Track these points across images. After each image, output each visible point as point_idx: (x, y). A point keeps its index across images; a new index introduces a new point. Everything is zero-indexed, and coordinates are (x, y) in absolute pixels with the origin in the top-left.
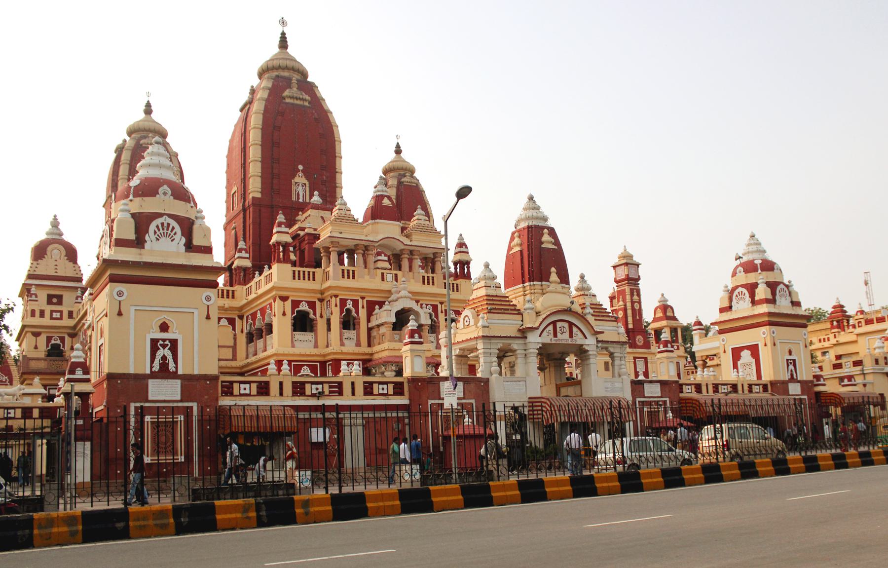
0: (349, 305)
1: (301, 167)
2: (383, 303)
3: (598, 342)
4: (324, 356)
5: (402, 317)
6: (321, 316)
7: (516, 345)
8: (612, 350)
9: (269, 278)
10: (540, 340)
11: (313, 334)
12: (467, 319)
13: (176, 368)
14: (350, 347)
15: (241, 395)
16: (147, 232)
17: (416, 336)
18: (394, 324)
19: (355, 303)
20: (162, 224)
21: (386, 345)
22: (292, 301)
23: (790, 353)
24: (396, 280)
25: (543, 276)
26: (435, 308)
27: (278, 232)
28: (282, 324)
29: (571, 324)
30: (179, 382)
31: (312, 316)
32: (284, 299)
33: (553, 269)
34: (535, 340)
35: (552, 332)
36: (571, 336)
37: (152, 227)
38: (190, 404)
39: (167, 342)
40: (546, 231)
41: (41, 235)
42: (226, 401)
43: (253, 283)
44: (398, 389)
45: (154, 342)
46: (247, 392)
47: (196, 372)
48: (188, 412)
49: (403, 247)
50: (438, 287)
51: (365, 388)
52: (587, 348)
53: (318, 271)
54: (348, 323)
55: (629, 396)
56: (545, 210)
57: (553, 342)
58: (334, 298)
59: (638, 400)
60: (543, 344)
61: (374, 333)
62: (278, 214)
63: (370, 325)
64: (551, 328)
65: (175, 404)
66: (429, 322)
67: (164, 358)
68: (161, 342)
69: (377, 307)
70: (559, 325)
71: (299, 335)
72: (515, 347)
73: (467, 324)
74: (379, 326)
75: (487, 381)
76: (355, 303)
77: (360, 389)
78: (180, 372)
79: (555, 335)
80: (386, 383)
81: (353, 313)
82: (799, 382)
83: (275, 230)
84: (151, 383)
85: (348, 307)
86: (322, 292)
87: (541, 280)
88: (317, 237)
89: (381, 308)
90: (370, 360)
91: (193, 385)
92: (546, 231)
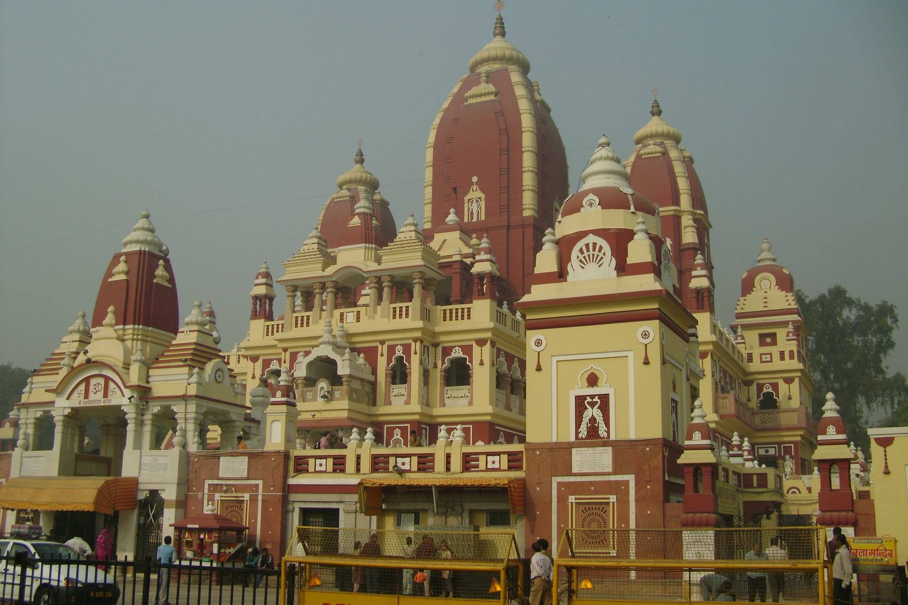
18: (306, 379)
23: (593, 380)
32: (254, 359)
35: (83, 392)
50: (413, 319)
57: (82, 405)
60: (72, 409)
64: (82, 387)
70: (93, 382)
82: (606, 443)
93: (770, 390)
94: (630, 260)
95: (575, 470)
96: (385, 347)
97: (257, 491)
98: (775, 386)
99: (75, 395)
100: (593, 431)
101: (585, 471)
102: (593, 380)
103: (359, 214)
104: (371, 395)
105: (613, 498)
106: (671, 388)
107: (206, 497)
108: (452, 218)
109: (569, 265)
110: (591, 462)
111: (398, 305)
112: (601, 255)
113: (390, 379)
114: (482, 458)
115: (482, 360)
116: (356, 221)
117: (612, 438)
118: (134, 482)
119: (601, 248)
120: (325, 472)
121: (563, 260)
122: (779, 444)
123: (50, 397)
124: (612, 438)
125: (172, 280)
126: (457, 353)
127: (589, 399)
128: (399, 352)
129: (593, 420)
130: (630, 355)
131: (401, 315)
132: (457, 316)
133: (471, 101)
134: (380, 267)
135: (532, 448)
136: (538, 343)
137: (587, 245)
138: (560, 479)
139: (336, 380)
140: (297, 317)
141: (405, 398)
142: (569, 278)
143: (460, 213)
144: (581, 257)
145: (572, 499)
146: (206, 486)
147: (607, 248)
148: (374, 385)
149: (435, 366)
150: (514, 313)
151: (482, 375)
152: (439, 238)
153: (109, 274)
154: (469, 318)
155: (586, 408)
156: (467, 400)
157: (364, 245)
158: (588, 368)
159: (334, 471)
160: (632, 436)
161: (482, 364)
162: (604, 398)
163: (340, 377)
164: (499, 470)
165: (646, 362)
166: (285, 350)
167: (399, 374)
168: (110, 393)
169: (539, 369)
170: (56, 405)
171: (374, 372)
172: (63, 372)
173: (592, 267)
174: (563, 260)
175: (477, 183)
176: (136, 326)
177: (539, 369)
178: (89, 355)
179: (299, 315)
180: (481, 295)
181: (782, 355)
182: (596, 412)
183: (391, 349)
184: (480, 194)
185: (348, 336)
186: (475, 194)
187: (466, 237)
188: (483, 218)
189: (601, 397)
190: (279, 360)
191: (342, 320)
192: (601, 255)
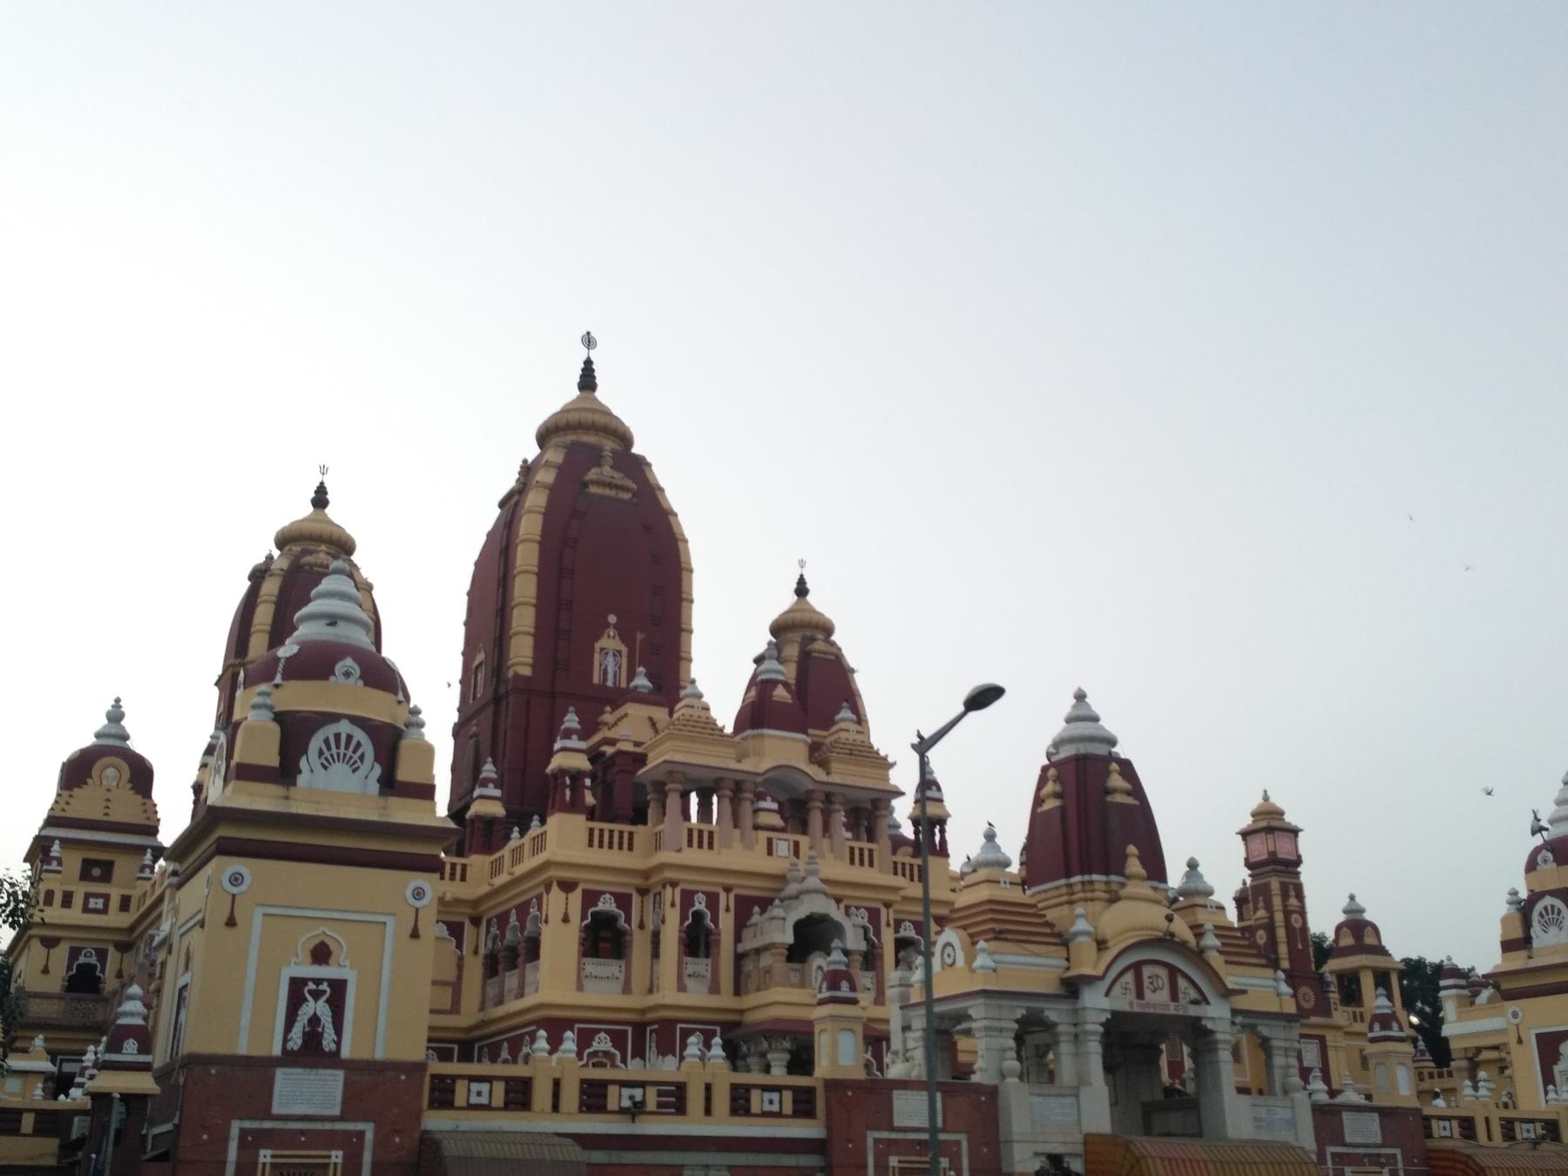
0: (700, 904)
1: (612, 619)
2: (770, 901)
3: (1235, 1012)
4: (643, 1011)
5: (812, 935)
6: (641, 926)
7: (1053, 1013)
8: (1265, 1031)
9: (539, 843)
10: (1106, 1004)
11: (623, 963)
12: (949, 950)
13: (338, 1043)
14: (697, 996)
15: (472, 1107)
16: (305, 751)
17: (845, 985)
18: (790, 948)
19: (712, 900)
20: (337, 736)
21: (777, 994)
22: (585, 892)
24: (797, 853)
25: (1112, 864)
26: (874, 915)
27: (564, 749)
28: (560, 939)
29: (1173, 972)
30: (340, 1075)
31: (622, 922)
33: (1132, 849)
34: (1097, 1004)
35: (1132, 986)
36: (1174, 996)
37: (316, 742)
38: (360, 1126)
39: (324, 986)
40: (1114, 766)
42: (436, 1121)
43: (506, 852)
44: (804, 1105)
45: (297, 985)
46: (484, 1100)
47: (379, 1055)
48: (352, 1144)
49: (810, 786)
50: (881, 871)
51: (734, 1099)
52: (1210, 1025)
53: (639, 829)
54: (697, 941)
55: (1307, 1139)
56: (1109, 724)
57: (1136, 1009)
58: (669, 889)
59: (1330, 1149)
60: (1115, 1014)
61: (748, 966)
62: (565, 713)
63: (741, 949)
64: (1129, 977)
65: (328, 1126)
66: (863, 946)
67: (315, 1020)
68: (311, 986)
69: (756, 909)
70: (1147, 971)
71: (592, 966)
72: (1052, 1016)
73: (949, 961)
74: (758, 951)
75: (993, 1092)
76: (712, 900)
77: (722, 1100)
78: (346, 1053)
79: (1140, 994)
80: (778, 1089)
81: (708, 922)
83: (557, 746)
84: (281, 1074)
85: (697, 907)
86: (646, 874)
87: (1107, 872)
88: (641, 759)
89: (763, 911)
90: (738, 1024)
91: (371, 1083)
92: (1114, 766)
97: (1396, 1163)
99: (1117, 990)
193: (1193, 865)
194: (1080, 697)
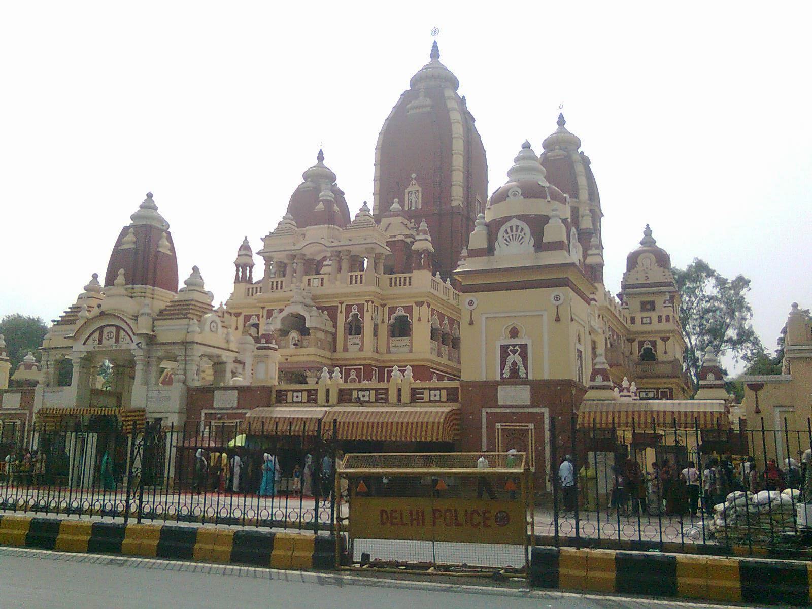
10: (83, 348)
18: (280, 330)
23: (514, 333)
36: (117, 341)
41: (635, 246)
60: (88, 352)
64: (97, 334)
70: (106, 330)
79: (100, 342)
82: (525, 382)
93: (649, 346)
94: (545, 240)
95: (500, 403)
96: (344, 306)
98: (654, 343)
99: (90, 341)
100: (514, 372)
101: (508, 404)
102: (514, 333)
103: (322, 201)
104: (332, 344)
105: (531, 426)
106: (577, 341)
107: (202, 423)
108: (396, 206)
109: (496, 243)
110: (513, 397)
111: (353, 274)
112: (522, 235)
113: (347, 332)
114: (426, 392)
115: (419, 318)
116: (321, 206)
117: (530, 378)
118: (142, 411)
119: (522, 229)
120: (301, 402)
121: (492, 237)
122: (657, 389)
123: (68, 343)
124: (530, 378)
125: (172, 249)
126: (401, 312)
127: (511, 348)
128: (355, 310)
129: (514, 364)
130: (545, 314)
131: (356, 282)
132: (400, 283)
133: (411, 112)
134: (341, 244)
135: (466, 385)
136: (471, 303)
137: (511, 227)
138: (489, 410)
139: (304, 331)
140: (272, 282)
141: (359, 346)
142: (496, 253)
143: (402, 203)
144: (506, 236)
145: (498, 425)
146: (203, 415)
147: (527, 230)
148: (334, 336)
149: (383, 322)
150: (445, 281)
151: (421, 331)
152: (385, 221)
153: (119, 242)
154: (410, 285)
155: (509, 355)
156: (407, 349)
157: (327, 225)
158: (510, 323)
159: (308, 402)
160: (546, 377)
161: (419, 320)
162: (524, 347)
163: (308, 329)
164: (440, 401)
165: (558, 320)
166: (263, 308)
167: (355, 328)
168: (120, 340)
169: (471, 323)
170: (74, 349)
171: (335, 326)
172: (80, 323)
173: (514, 244)
174: (492, 237)
175: (415, 179)
176: (143, 286)
177: (471, 323)
178: (103, 308)
179: (275, 280)
180: (419, 267)
181: (660, 318)
182: (517, 358)
183: (349, 307)
184: (417, 188)
185: (314, 298)
186: (414, 187)
187: (406, 222)
188: (420, 207)
189: (521, 346)
190: (258, 316)
191: (309, 284)
192: (522, 235)
193: (195, 269)
194: (150, 196)
